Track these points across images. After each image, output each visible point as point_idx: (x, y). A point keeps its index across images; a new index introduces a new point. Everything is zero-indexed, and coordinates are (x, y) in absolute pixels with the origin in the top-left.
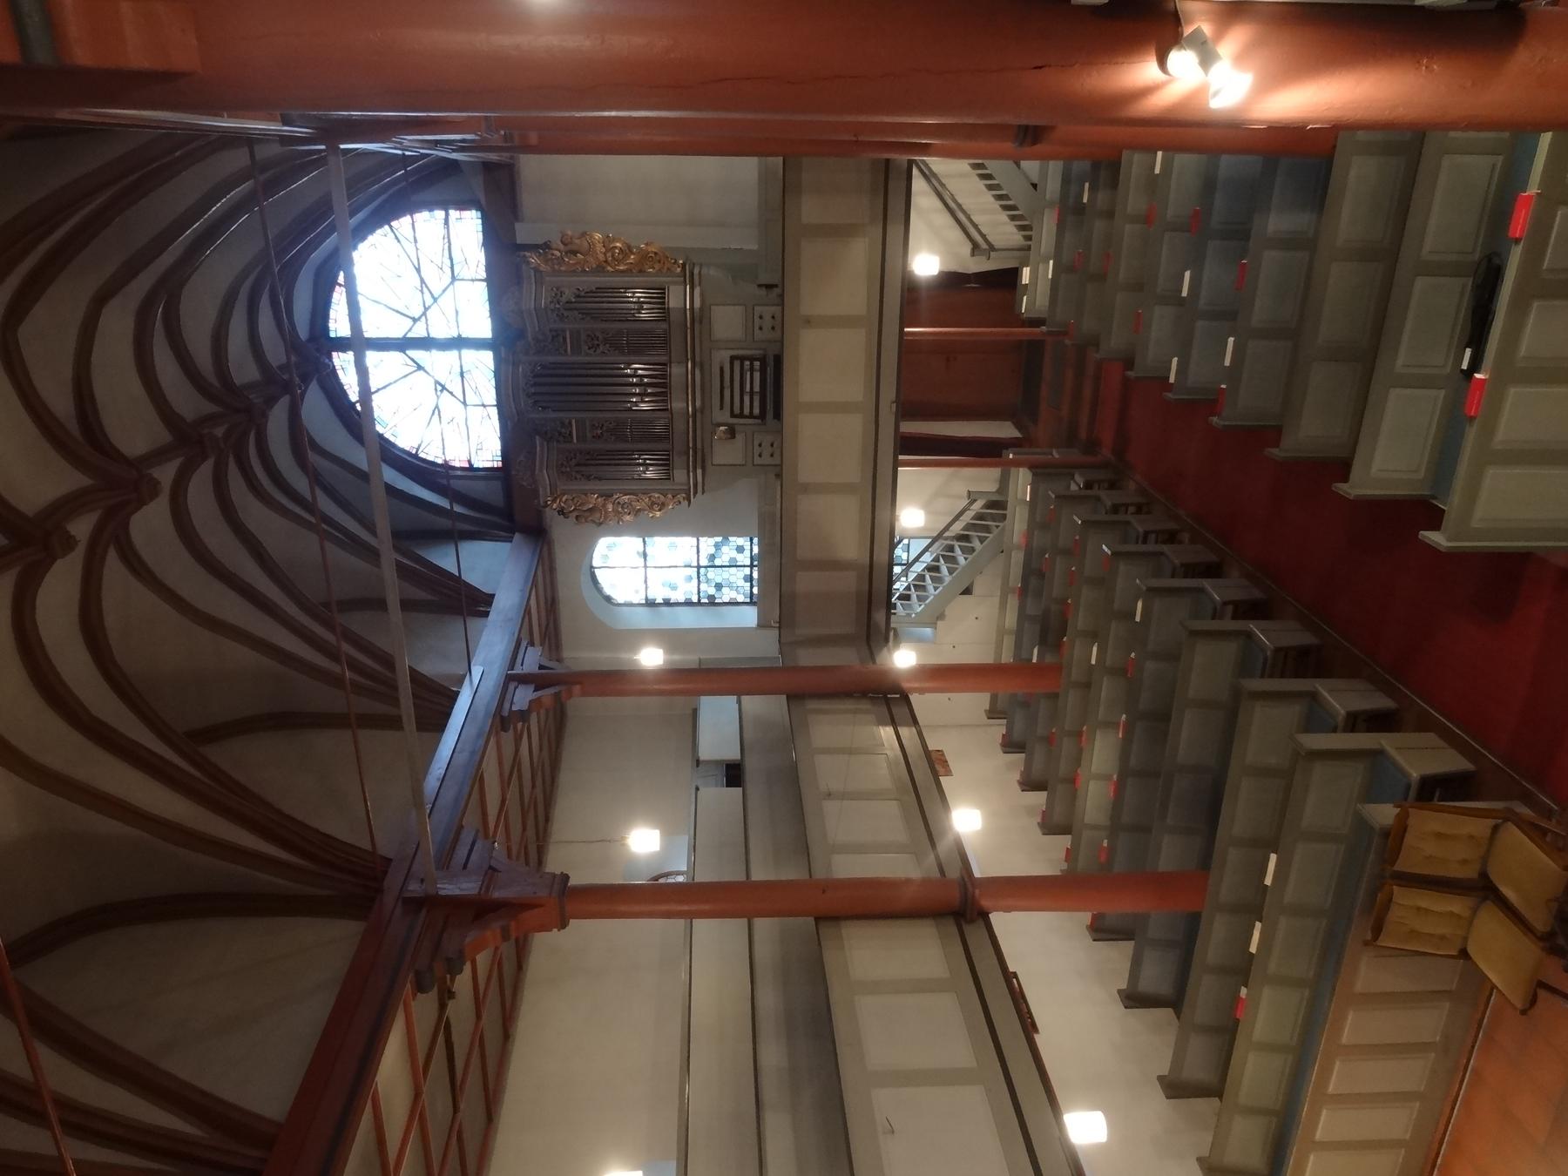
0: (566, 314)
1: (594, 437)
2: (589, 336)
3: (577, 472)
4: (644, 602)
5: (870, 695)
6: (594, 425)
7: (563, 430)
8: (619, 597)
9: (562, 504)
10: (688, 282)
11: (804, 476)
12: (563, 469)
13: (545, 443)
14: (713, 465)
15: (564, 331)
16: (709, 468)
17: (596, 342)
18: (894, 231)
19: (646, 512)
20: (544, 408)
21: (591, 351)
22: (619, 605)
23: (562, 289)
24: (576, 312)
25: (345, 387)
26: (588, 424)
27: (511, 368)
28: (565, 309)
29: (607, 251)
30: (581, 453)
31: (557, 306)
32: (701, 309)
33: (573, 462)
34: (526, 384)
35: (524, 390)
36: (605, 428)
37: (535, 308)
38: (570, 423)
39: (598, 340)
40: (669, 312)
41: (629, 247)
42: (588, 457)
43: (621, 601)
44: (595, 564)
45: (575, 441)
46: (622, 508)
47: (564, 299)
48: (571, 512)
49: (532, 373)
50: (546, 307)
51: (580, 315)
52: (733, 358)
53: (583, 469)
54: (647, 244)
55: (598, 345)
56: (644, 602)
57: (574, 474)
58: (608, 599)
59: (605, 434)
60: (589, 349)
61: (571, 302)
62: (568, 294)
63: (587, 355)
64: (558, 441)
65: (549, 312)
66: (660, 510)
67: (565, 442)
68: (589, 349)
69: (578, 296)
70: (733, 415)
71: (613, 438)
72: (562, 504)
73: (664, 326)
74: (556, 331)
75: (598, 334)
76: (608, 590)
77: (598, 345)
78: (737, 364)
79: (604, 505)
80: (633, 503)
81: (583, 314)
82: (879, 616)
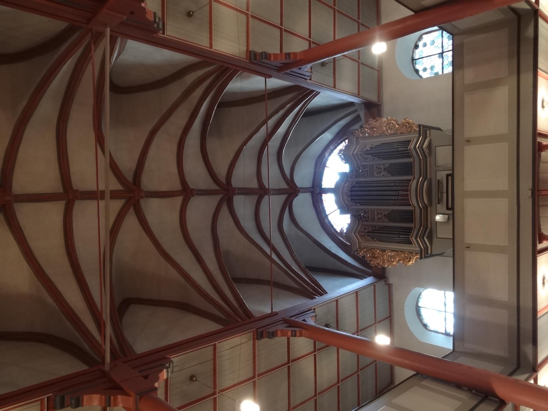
0: (366, 156)
1: (378, 219)
2: (377, 167)
3: (368, 236)
4: (444, 332)
5: (474, 391)
6: (378, 213)
7: (365, 215)
8: (431, 327)
9: (364, 253)
10: (422, 135)
11: (470, 238)
12: (361, 234)
13: (357, 221)
14: (437, 237)
15: (366, 165)
16: (435, 240)
17: (381, 170)
18: (527, 78)
19: (401, 262)
20: (356, 203)
21: (378, 175)
22: (431, 331)
23: (366, 146)
24: (370, 155)
25: (325, 209)
26: (376, 212)
27: (344, 183)
28: (365, 154)
29: (387, 125)
30: (371, 227)
31: (362, 152)
32: (430, 146)
33: (367, 230)
34: (348, 191)
35: (346, 193)
36: (383, 214)
37: (352, 154)
38: (368, 212)
39: (381, 169)
40: (411, 151)
41: (397, 122)
42: (374, 229)
43: (431, 329)
44: (420, 305)
45: (370, 220)
46: (391, 258)
47: (365, 150)
48: (368, 257)
49: (351, 185)
50: (356, 154)
51: (372, 157)
52: (448, 176)
53: (370, 234)
54: (405, 119)
55: (381, 172)
56: (444, 332)
57: (366, 236)
58: (425, 326)
59: (383, 217)
60: (377, 174)
61: (368, 151)
62: (368, 147)
63: (376, 177)
64: (363, 221)
65: (359, 156)
66: (409, 262)
67: (366, 221)
68: (377, 174)
69: (372, 148)
70: (448, 208)
71: (387, 219)
72: (364, 253)
73: (411, 160)
74: (364, 166)
75: (381, 166)
76: (426, 321)
77: (381, 172)
78: (450, 178)
79: (382, 256)
80: (396, 256)
81: (373, 156)
82: (528, 349)
